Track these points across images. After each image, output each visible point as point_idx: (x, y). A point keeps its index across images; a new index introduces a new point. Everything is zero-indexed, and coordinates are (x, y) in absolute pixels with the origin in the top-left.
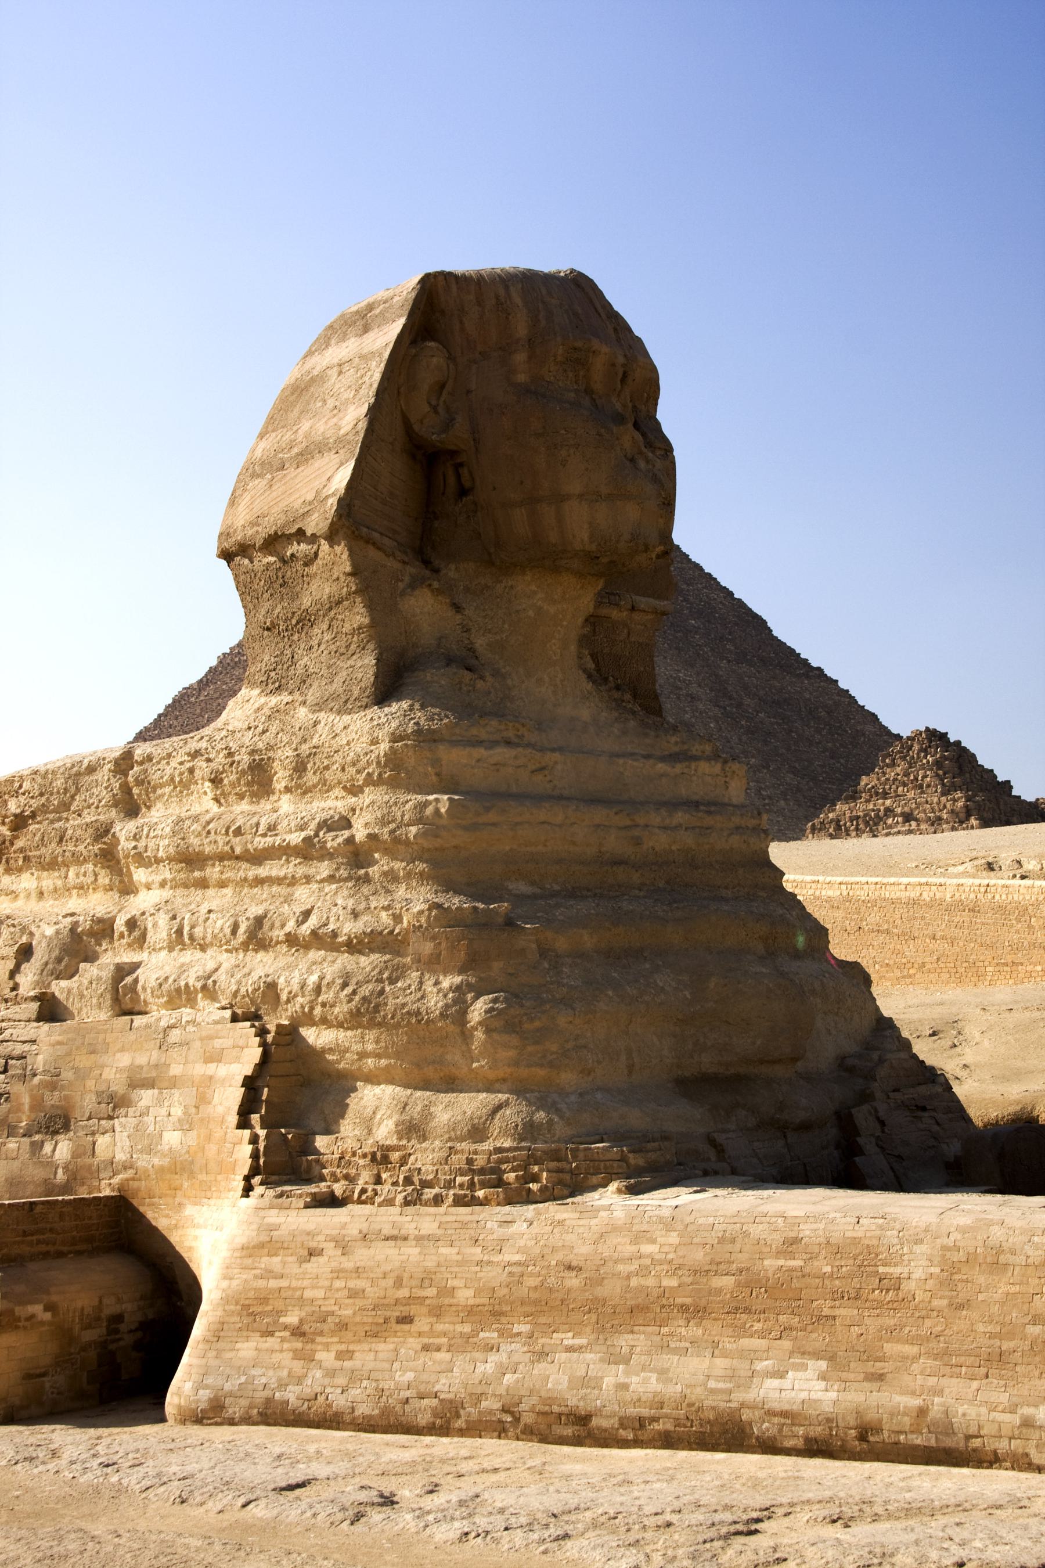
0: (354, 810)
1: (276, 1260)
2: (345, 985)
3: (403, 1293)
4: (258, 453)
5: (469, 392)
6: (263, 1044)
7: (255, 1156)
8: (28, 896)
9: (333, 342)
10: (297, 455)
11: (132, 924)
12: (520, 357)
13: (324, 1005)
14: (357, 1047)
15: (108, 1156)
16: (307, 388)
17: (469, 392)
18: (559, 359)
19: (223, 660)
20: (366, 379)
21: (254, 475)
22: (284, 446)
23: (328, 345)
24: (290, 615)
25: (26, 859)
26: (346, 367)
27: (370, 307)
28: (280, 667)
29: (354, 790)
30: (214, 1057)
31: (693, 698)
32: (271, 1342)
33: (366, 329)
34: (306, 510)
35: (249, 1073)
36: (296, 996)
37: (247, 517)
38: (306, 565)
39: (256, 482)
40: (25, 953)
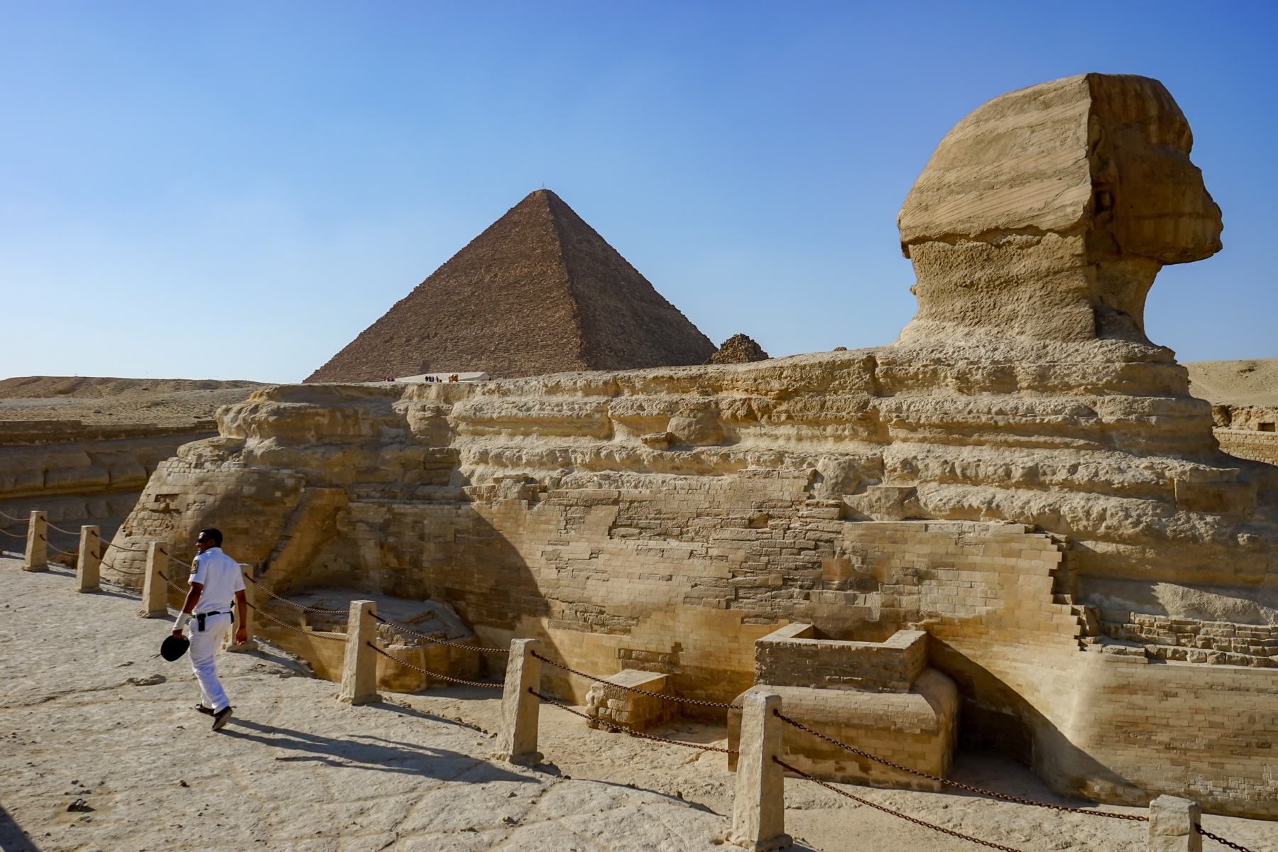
0: (1095, 404)
1: (1138, 699)
2: (1127, 516)
3: (1258, 727)
4: (951, 177)
6: (1059, 550)
7: (1080, 622)
8: (788, 439)
11: (906, 463)
12: (1153, 128)
13: (1108, 528)
14: (1139, 556)
15: (913, 607)
17: (1116, 147)
19: (416, 289)
20: (1070, 133)
21: (951, 192)
25: (789, 417)
29: (1097, 390)
30: (1018, 554)
31: (624, 316)
32: (1148, 752)
35: (1055, 567)
36: (1080, 519)
38: (1021, 248)
40: (816, 476)
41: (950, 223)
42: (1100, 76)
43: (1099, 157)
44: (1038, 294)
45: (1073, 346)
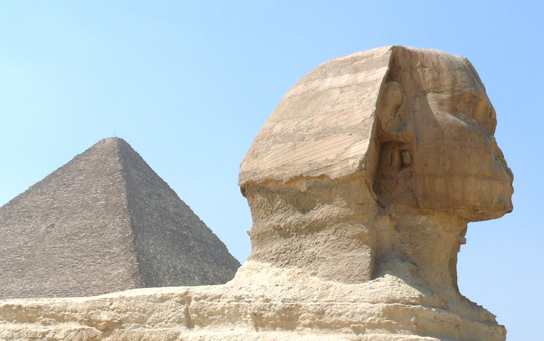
5: (414, 111)
9: (330, 74)
10: (316, 134)
16: (314, 97)
17: (414, 111)
18: (466, 101)
21: (274, 143)
22: (302, 127)
23: (326, 76)
24: (301, 223)
26: (346, 89)
27: (355, 60)
28: (289, 251)
33: (356, 70)
34: (328, 164)
37: (274, 165)
39: (279, 146)
41: (270, 170)
42: (404, 49)
43: (401, 119)
44: (332, 238)
45: (350, 287)
